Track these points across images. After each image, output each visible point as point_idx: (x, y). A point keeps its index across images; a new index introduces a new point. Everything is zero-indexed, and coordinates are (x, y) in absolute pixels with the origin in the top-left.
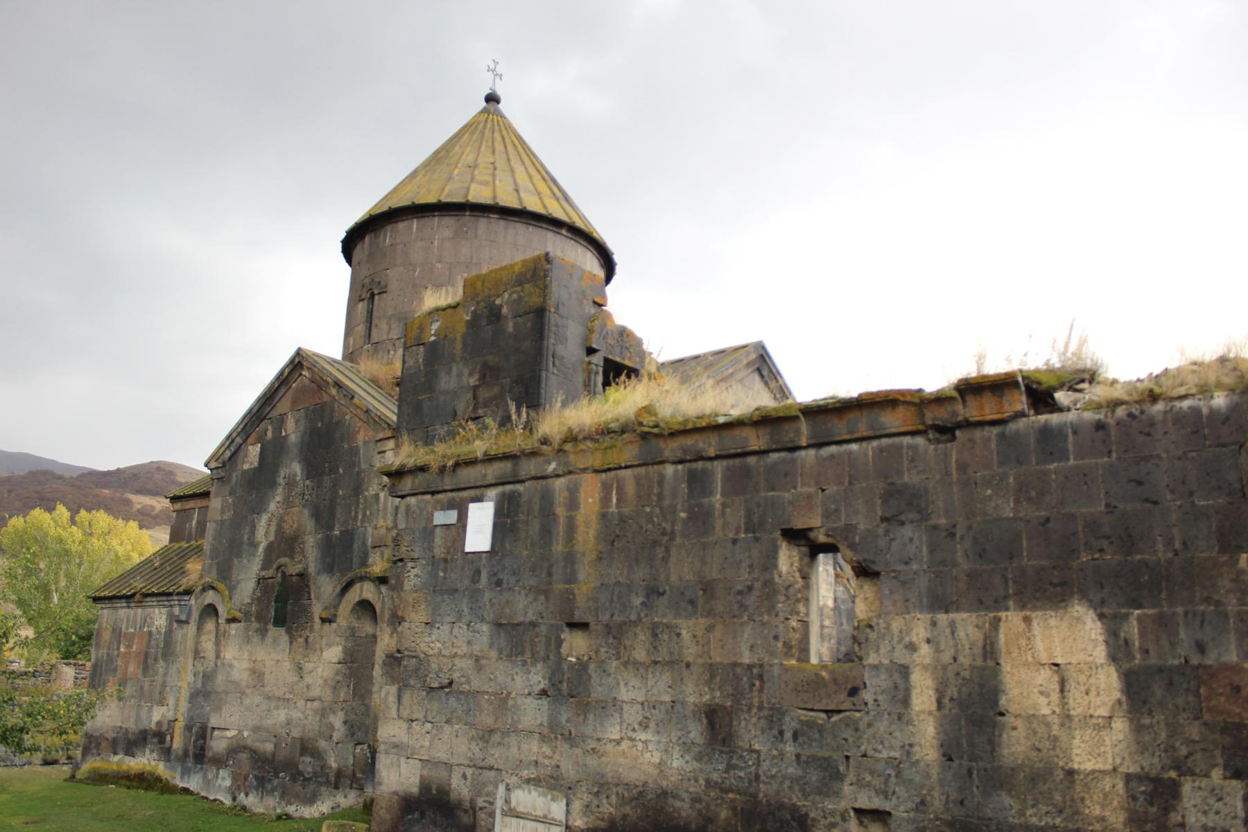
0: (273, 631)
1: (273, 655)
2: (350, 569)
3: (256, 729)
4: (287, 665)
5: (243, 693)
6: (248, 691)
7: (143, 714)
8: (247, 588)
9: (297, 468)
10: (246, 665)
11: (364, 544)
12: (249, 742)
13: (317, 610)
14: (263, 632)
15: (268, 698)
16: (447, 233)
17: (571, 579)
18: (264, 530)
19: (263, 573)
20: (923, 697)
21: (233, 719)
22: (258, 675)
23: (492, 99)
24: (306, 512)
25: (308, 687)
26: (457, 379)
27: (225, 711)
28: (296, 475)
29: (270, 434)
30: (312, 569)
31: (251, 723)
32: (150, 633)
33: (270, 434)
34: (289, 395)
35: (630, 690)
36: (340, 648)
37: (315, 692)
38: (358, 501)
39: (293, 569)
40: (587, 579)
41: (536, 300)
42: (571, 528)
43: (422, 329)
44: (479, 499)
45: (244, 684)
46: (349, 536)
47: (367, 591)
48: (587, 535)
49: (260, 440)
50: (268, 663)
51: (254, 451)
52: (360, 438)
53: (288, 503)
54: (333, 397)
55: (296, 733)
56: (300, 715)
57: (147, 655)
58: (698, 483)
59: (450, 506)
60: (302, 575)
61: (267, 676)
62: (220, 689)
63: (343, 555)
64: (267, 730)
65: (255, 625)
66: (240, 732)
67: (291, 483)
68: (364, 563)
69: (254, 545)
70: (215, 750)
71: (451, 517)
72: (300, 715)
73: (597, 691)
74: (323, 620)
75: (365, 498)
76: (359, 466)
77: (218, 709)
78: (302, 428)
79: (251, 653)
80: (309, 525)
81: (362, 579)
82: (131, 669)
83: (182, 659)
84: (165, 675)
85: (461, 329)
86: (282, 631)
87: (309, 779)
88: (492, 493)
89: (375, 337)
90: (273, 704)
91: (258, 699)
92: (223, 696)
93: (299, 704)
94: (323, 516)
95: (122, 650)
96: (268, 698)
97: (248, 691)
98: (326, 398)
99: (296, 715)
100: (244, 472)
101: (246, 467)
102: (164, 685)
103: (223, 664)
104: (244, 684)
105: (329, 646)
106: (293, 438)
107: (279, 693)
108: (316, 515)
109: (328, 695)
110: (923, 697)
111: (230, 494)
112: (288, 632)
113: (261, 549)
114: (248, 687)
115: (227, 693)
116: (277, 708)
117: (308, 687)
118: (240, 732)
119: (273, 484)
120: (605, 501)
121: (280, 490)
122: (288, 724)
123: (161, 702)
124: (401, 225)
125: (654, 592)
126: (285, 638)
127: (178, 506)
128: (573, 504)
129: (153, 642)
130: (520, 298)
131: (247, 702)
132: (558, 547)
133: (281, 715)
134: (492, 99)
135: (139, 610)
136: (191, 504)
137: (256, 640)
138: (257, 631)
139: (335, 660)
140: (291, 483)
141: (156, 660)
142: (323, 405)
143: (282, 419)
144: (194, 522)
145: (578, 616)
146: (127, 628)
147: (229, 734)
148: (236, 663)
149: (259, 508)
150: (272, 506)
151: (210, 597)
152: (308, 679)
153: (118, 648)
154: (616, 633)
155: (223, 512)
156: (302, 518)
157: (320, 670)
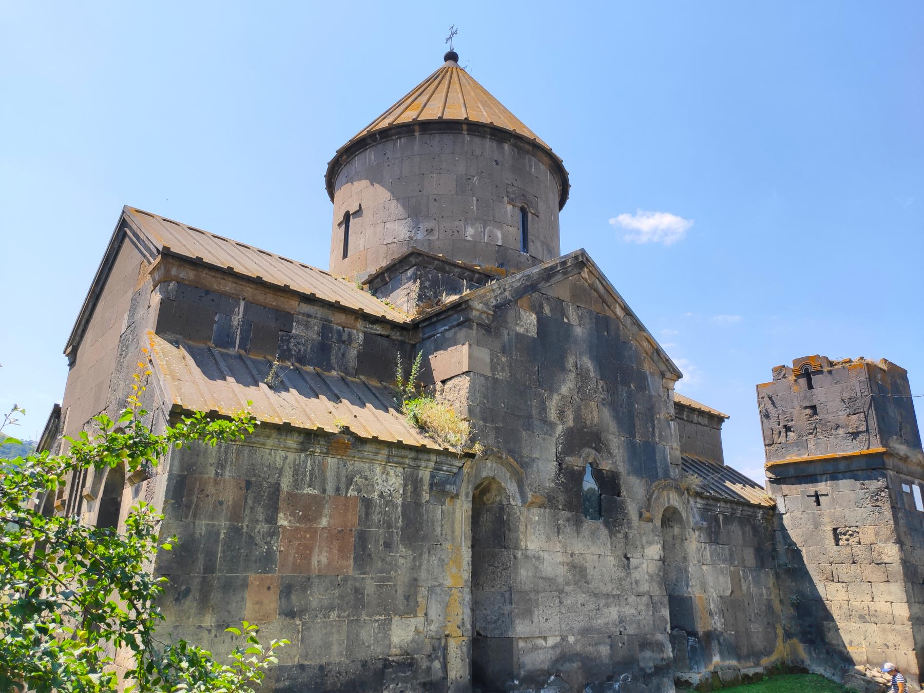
0: (589, 524)
3: (585, 632)
4: (611, 560)
5: (561, 591)
6: (567, 589)
7: (367, 634)
8: (545, 469)
9: (588, 363)
10: (560, 558)
11: (665, 458)
12: (578, 648)
14: (578, 524)
15: (596, 595)
19: (569, 459)
21: (551, 624)
22: (579, 571)
23: (452, 57)
24: (606, 413)
25: (637, 582)
27: (538, 615)
28: (588, 370)
30: (622, 469)
31: (577, 626)
32: (368, 503)
33: (547, 310)
36: (660, 546)
37: (645, 587)
38: (653, 421)
45: (560, 580)
50: (589, 557)
54: (618, 318)
55: (631, 630)
56: (633, 611)
57: (362, 539)
61: (590, 571)
62: (527, 588)
64: (599, 631)
65: (566, 514)
66: (564, 638)
70: (529, 667)
72: (633, 611)
75: (659, 420)
76: (650, 391)
77: (528, 613)
78: (588, 326)
79: (565, 546)
80: (613, 426)
82: (320, 558)
83: (447, 545)
84: (415, 568)
86: (600, 523)
87: (650, 675)
90: (602, 602)
91: (582, 598)
92: (532, 596)
93: (630, 600)
95: (283, 521)
96: (596, 595)
97: (568, 589)
98: (609, 313)
99: (629, 611)
100: (518, 334)
102: (414, 583)
103: (527, 557)
104: (560, 580)
105: (650, 543)
111: (504, 350)
112: (606, 524)
113: (560, 429)
114: (567, 584)
115: (537, 592)
116: (607, 606)
117: (637, 582)
118: (564, 638)
122: (621, 622)
123: (410, 609)
126: (604, 531)
127: (188, 274)
129: (375, 518)
131: (568, 601)
133: (613, 613)
134: (452, 57)
136: (228, 286)
137: (569, 530)
138: (568, 520)
139: (657, 557)
140: (582, 376)
141: (388, 545)
142: (607, 319)
144: (237, 319)
146: (296, 484)
147: (551, 642)
148: (546, 556)
150: (564, 390)
152: (636, 575)
153: (271, 520)
156: (599, 415)
157: (644, 566)
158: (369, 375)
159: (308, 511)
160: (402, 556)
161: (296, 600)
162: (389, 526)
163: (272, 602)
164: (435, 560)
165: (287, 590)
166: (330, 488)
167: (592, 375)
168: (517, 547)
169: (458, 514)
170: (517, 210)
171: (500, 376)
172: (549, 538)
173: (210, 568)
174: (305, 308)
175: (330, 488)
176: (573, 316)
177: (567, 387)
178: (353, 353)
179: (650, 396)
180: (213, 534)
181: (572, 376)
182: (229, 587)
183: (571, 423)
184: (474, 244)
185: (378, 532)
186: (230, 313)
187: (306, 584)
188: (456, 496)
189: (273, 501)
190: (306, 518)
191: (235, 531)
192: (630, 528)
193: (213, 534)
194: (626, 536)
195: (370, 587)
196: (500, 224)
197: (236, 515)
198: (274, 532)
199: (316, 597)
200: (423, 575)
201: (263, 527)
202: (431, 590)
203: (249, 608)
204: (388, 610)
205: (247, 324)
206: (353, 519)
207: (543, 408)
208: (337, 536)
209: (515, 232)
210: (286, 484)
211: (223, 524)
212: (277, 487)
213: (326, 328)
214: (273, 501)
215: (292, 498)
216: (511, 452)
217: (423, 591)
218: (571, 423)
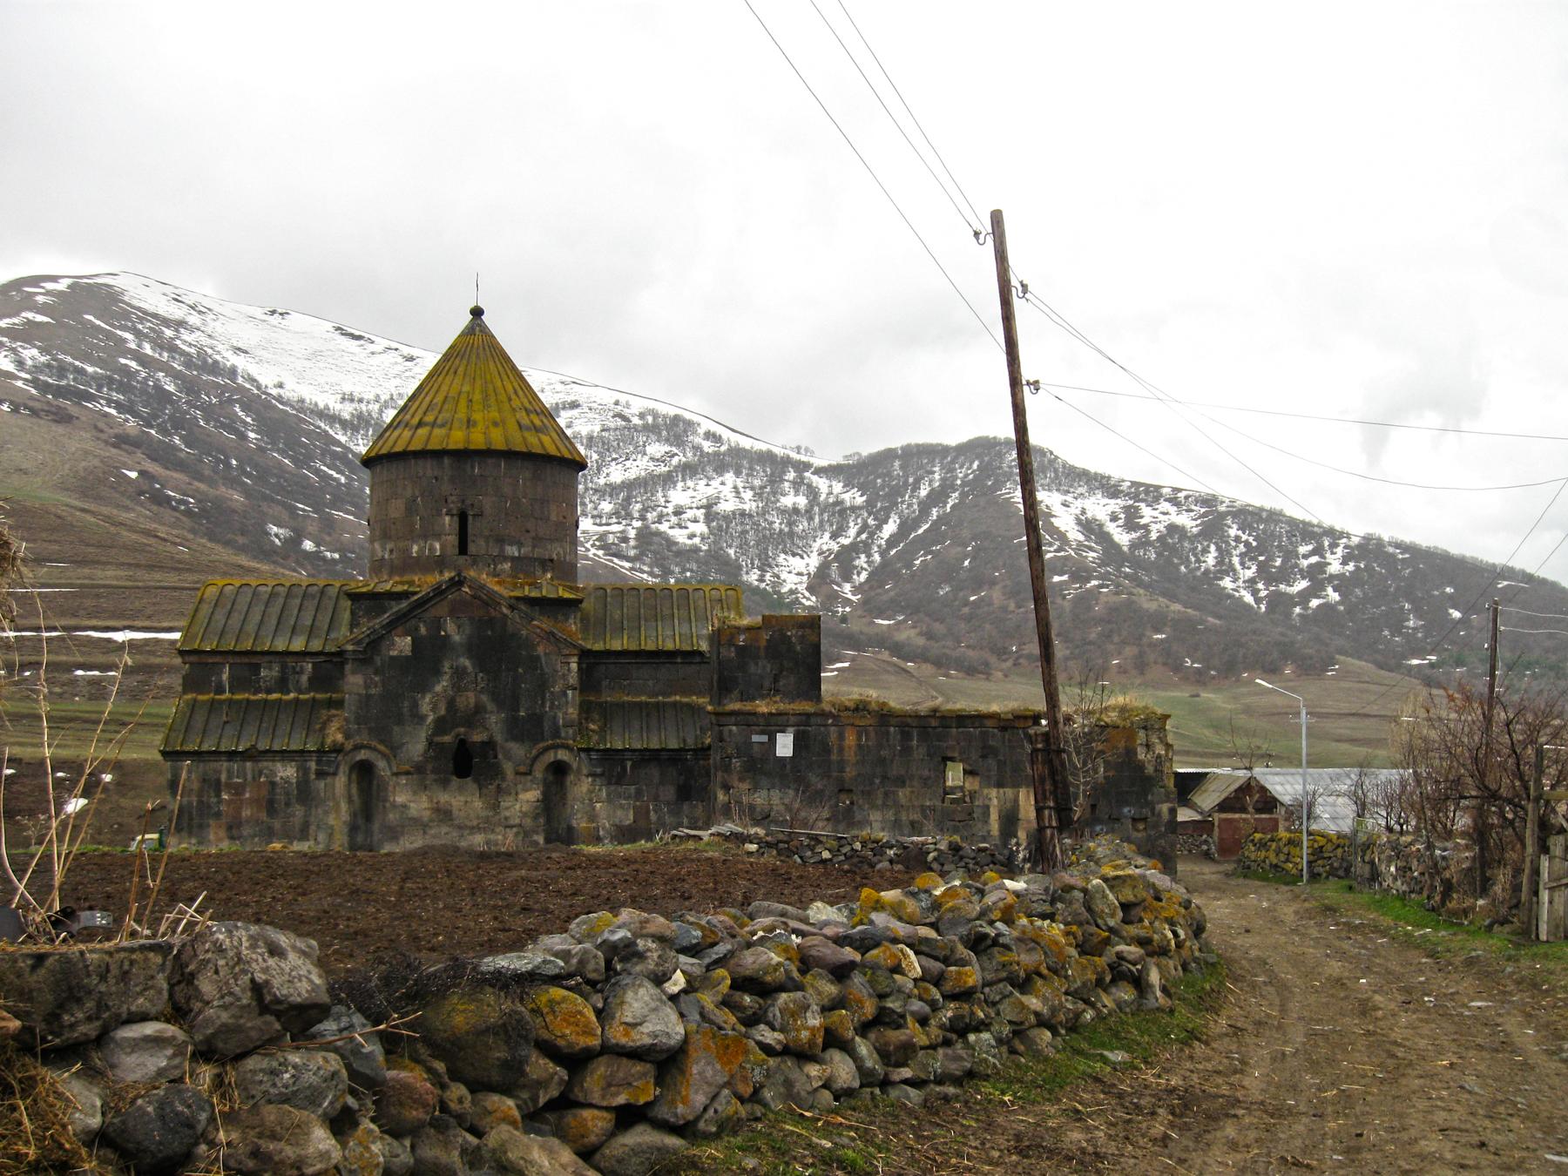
1: (465, 800)
2: (543, 739)
8: (416, 746)
9: (466, 662)
10: (426, 805)
13: (508, 768)
15: (460, 827)
16: (528, 474)
17: (842, 770)
18: (428, 706)
19: (438, 739)
20: (994, 816)
23: (477, 312)
24: (484, 698)
26: (761, 668)
28: (465, 668)
29: (423, 630)
30: (499, 738)
32: (273, 784)
33: (423, 630)
34: (445, 603)
35: (875, 816)
39: (478, 737)
40: (850, 772)
41: (813, 638)
42: (841, 749)
43: (732, 637)
44: (783, 732)
46: (536, 720)
47: (562, 755)
48: (850, 755)
49: (412, 631)
51: (403, 644)
52: (540, 650)
53: (457, 687)
58: (906, 736)
59: (762, 733)
60: (490, 745)
63: (530, 729)
67: (459, 673)
68: (556, 733)
69: (423, 718)
71: (764, 738)
73: (858, 817)
74: (517, 773)
79: (430, 799)
81: (556, 747)
82: (246, 813)
85: (763, 644)
88: (791, 729)
89: (472, 548)
90: (466, 832)
94: (508, 702)
96: (460, 827)
98: (493, 613)
101: (394, 653)
106: (457, 638)
107: (475, 823)
108: (495, 697)
109: (528, 822)
110: (994, 816)
112: (476, 781)
113: (430, 718)
117: (506, 818)
119: (437, 672)
120: (859, 739)
121: (446, 677)
124: (490, 461)
125: (885, 778)
127: (193, 658)
128: (841, 737)
130: (803, 636)
132: (834, 757)
134: (477, 312)
135: (249, 764)
136: (218, 659)
140: (459, 673)
143: (437, 624)
144: (225, 676)
145: (847, 786)
146: (230, 776)
149: (424, 688)
150: (438, 688)
151: (363, 755)
153: (218, 795)
154: (868, 794)
155: (367, 687)
158: (317, 691)
159: (238, 790)
160: (298, 811)
161: (235, 832)
162: (287, 794)
163: (222, 833)
164: (320, 811)
165: (230, 828)
166: (249, 777)
167: (470, 669)
168: (385, 800)
169: (338, 784)
170: (456, 519)
171: (373, 691)
172: (415, 793)
173: (191, 819)
174: (267, 658)
175: (249, 777)
176: (450, 627)
177: (442, 685)
178: (304, 678)
179: (542, 674)
180: (190, 803)
181: (446, 677)
182: (201, 826)
183: (443, 712)
184: (418, 558)
185: (281, 798)
186: (220, 673)
187: (239, 825)
188: (335, 774)
189: (217, 787)
190: (237, 794)
191: (200, 802)
192: (504, 779)
193: (190, 803)
194: (499, 789)
195: (277, 825)
196: (437, 536)
197: (200, 794)
198: (220, 801)
199: (246, 831)
200: (312, 819)
201: (214, 800)
202: (318, 827)
203: (212, 837)
204: (289, 837)
205: (231, 677)
206: (264, 792)
207: (415, 705)
208: (255, 801)
209: (453, 539)
210: (223, 777)
211: (194, 799)
212: (218, 781)
213: (284, 668)
214: (217, 787)
215: (229, 786)
216: (381, 742)
217: (313, 828)
218: (443, 712)
